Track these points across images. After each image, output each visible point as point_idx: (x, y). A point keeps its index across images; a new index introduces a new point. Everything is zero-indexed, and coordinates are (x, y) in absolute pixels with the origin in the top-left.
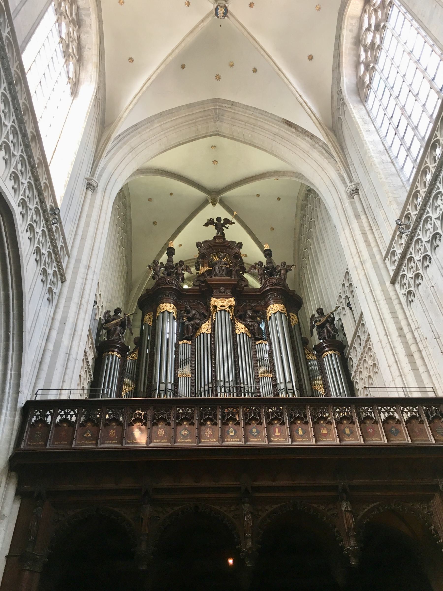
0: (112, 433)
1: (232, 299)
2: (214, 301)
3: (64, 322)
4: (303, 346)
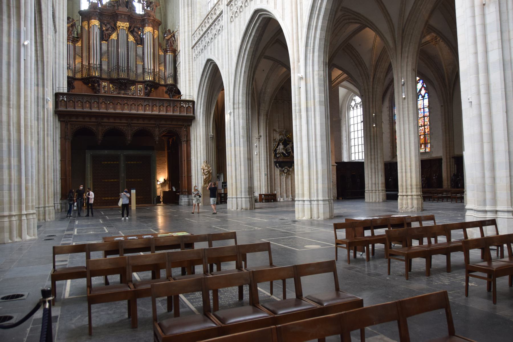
0: (88, 105)
1: (128, 23)
2: (119, 24)
4: (159, 47)
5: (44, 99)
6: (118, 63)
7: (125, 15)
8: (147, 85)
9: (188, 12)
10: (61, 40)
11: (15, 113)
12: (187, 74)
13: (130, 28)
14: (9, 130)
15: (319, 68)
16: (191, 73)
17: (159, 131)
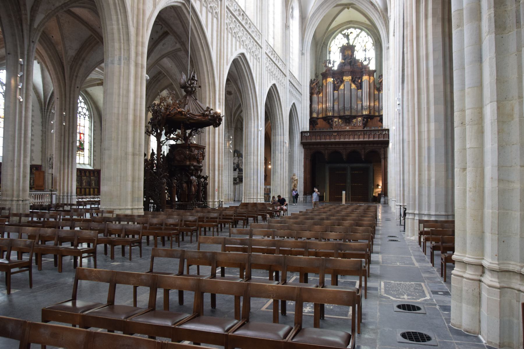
0: (319, 138)
1: (350, 77)
2: (345, 78)
3: (304, 107)
5: (284, 142)
6: (344, 105)
7: (348, 71)
8: (364, 118)
13: (352, 78)
14: (254, 165)
17: (364, 152)
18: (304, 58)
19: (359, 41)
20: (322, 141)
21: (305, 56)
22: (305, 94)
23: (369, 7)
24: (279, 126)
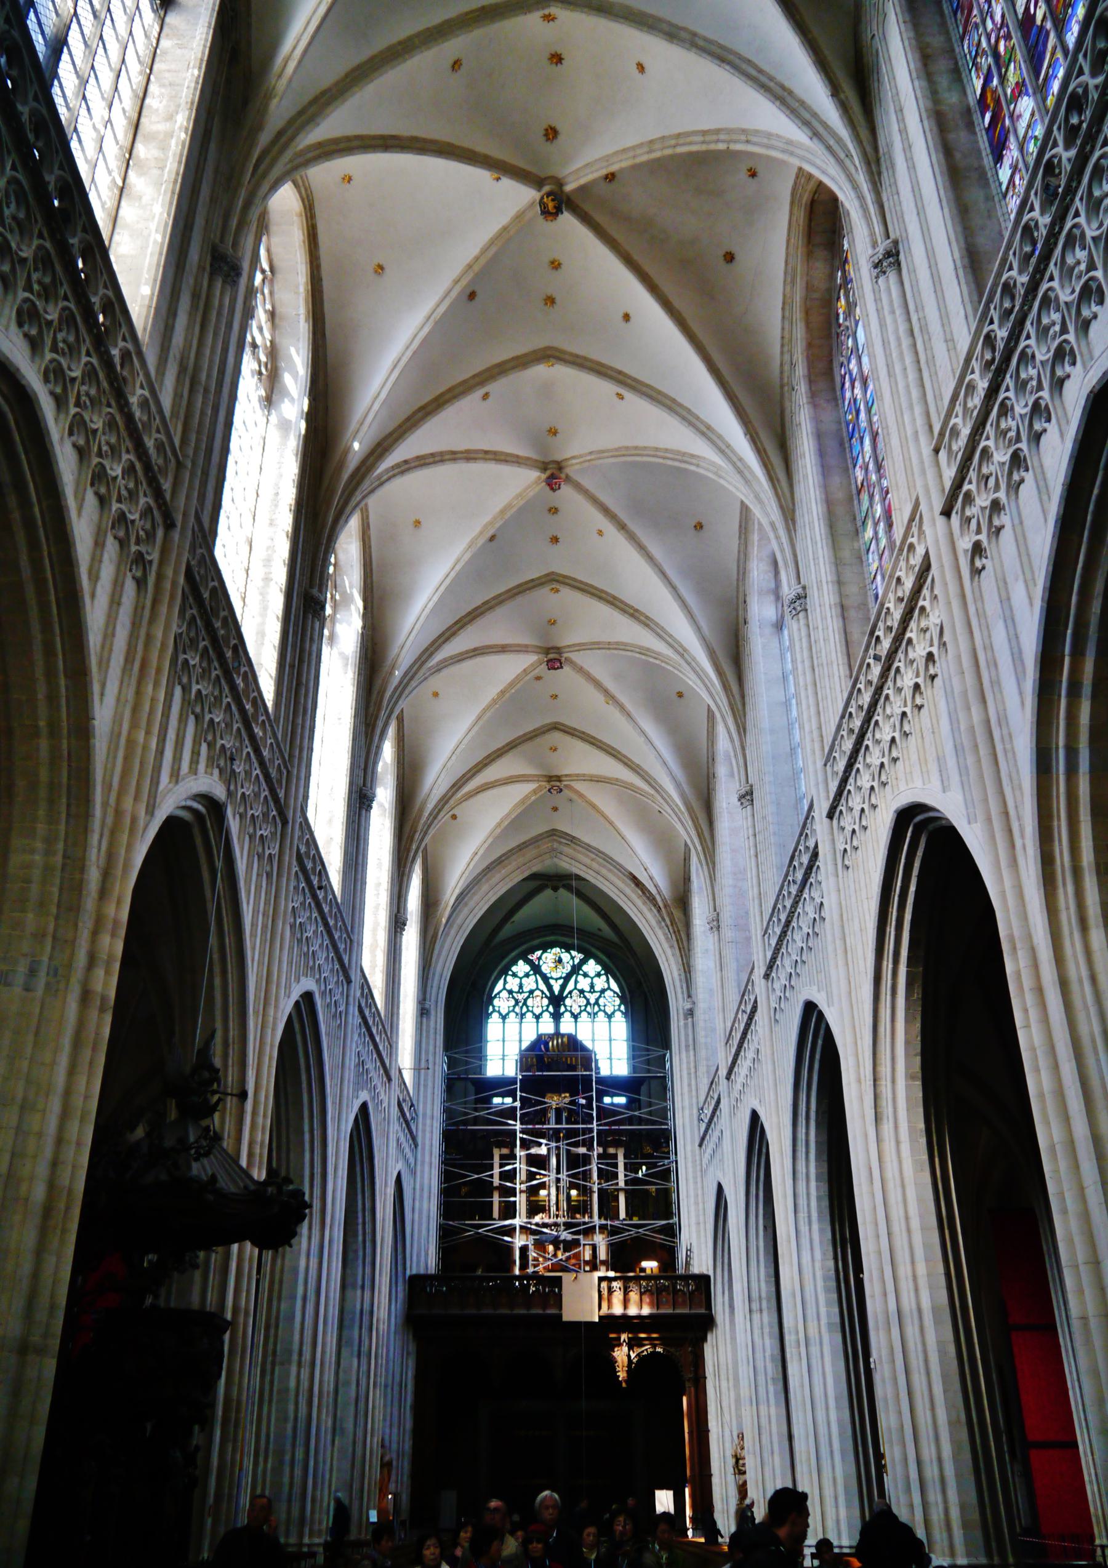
3: (422, 1190)
9: (688, 1063)
10: (427, 1159)
11: (307, 1375)
12: (692, 1208)
15: (824, 1254)
16: (701, 1206)
18: (428, 1026)
19: (579, 987)
20: (468, 1311)
21: (432, 1018)
22: (427, 1142)
23: (628, 891)
24: (361, 1253)
